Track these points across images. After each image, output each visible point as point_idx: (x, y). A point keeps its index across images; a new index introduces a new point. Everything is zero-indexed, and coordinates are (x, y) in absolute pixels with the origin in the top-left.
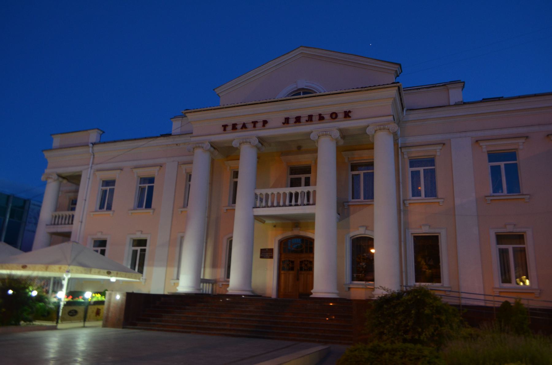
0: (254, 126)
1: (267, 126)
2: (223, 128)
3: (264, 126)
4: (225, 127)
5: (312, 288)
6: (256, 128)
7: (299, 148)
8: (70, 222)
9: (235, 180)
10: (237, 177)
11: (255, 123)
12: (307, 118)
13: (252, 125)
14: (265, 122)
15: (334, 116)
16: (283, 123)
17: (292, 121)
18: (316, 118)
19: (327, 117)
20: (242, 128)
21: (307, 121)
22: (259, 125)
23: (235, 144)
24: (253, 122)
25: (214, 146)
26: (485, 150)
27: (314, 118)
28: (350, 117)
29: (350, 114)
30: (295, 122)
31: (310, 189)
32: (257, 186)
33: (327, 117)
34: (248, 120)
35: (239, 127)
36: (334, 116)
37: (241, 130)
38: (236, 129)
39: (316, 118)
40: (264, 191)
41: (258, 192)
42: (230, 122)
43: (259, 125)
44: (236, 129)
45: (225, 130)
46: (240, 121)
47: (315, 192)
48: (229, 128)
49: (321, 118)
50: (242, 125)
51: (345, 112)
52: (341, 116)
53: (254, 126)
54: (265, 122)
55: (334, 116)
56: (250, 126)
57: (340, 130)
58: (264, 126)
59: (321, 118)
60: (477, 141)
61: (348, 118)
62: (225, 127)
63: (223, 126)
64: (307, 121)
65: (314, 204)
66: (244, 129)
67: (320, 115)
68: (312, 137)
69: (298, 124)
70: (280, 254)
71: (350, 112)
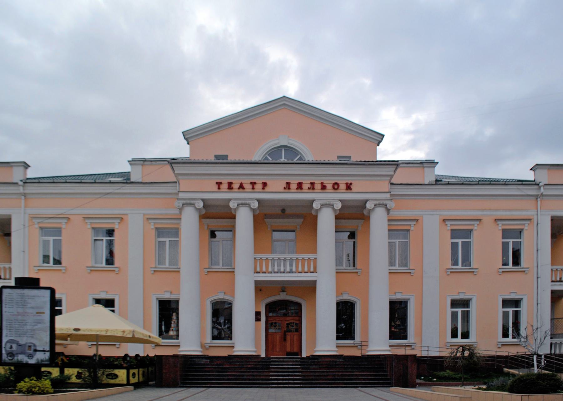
0: (253, 188)
1: (267, 189)
2: (217, 186)
3: (263, 189)
4: (219, 184)
5: (315, 347)
8: (8, 277)
11: (253, 184)
12: (309, 186)
13: (251, 186)
14: (265, 185)
15: (336, 186)
16: (285, 188)
17: (294, 186)
18: (318, 186)
19: (329, 186)
20: (239, 188)
21: (309, 188)
22: (259, 187)
23: (233, 205)
24: (251, 183)
25: (207, 204)
27: (316, 186)
28: (351, 189)
29: (352, 187)
30: (297, 189)
31: (312, 256)
32: (256, 251)
33: (329, 186)
34: (246, 182)
35: (236, 186)
37: (237, 190)
38: (232, 188)
39: (318, 186)
41: (259, 256)
43: (259, 187)
44: (232, 188)
45: (219, 188)
47: (316, 259)
48: (225, 186)
49: (324, 187)
50: (238, 185)
51: (347, 184)
52: (343, 187)
53: (253, 188)
55: (336, 187)
56: (248, 186)
57: (341, 200)
58: (263, 189)
61: (349, 191)
63: (217, 183)
64: (309, 188)
65: (315, 271)
66: (241, 190)
67: (322, 183)
68: (316, 205)
69: (299, 191)
71: (351, 184)
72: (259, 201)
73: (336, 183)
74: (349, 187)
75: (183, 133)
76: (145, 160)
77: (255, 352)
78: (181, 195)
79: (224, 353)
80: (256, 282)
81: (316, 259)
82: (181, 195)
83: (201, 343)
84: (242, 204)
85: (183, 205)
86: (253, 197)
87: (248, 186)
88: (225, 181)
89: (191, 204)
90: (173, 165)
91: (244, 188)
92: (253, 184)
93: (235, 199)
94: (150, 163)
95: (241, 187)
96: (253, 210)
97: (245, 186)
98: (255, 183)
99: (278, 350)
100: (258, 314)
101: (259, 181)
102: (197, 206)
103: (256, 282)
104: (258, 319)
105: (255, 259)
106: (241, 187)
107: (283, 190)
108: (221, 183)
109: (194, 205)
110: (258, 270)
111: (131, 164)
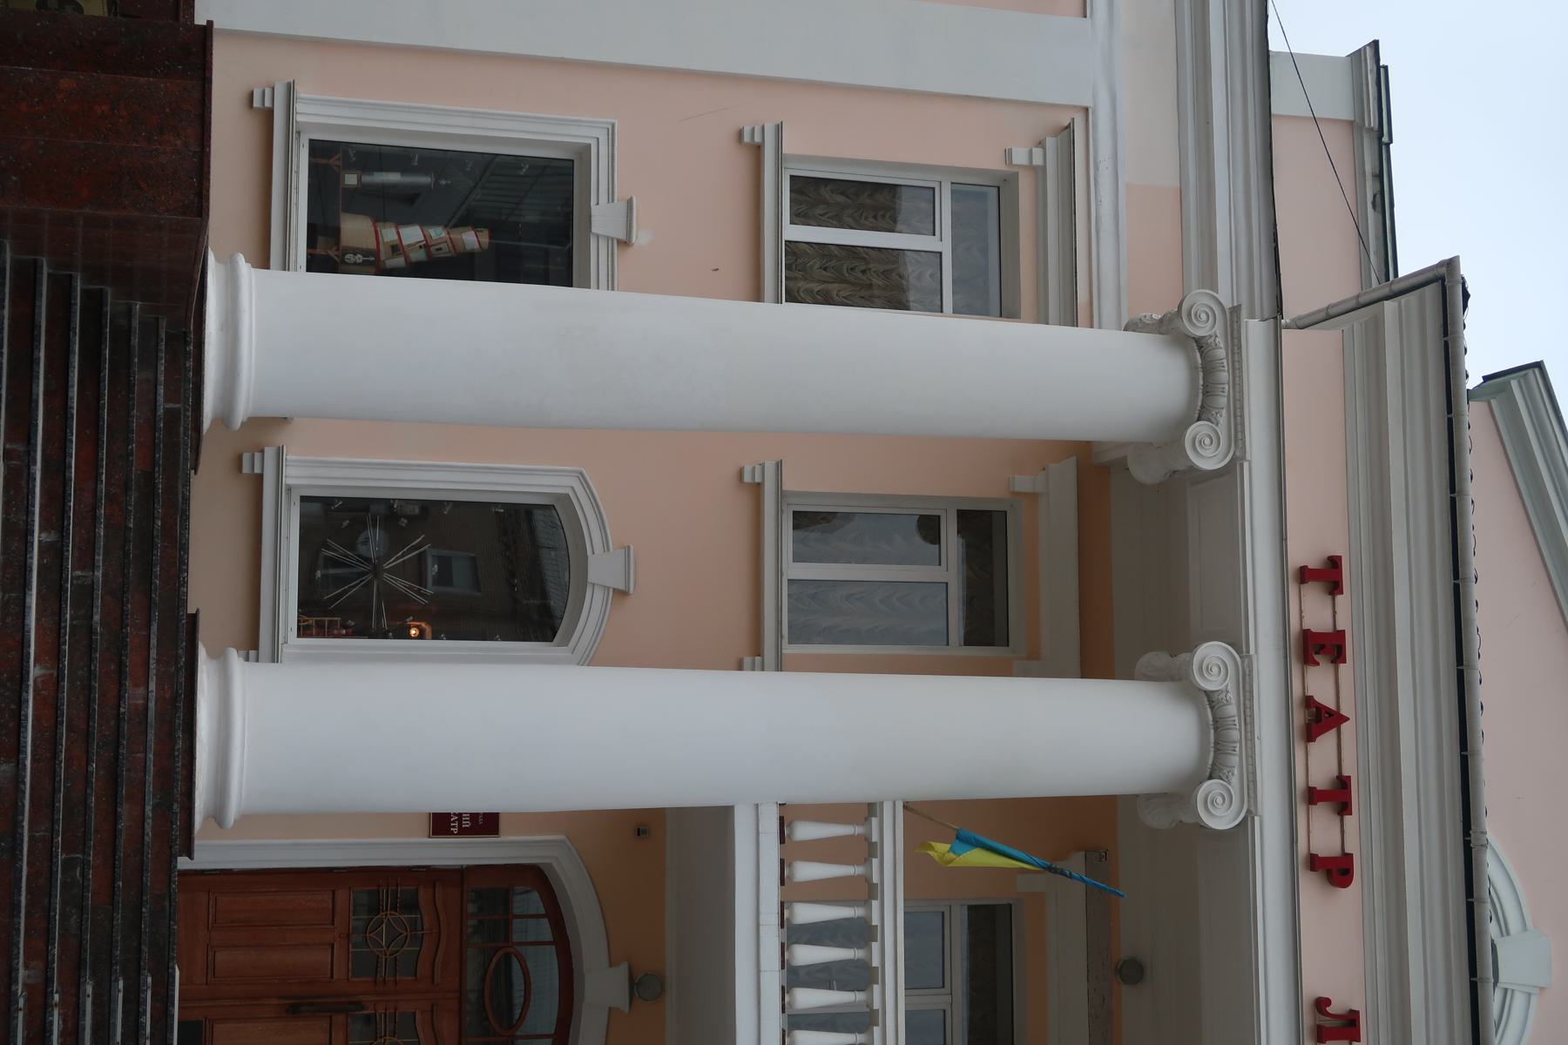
0: (1313, 796)
1: (1310, 886)
2: (1314, 562)
4: (1328, 576)
6: (1301, 810)
7: (1133, 971)
13: (1321, 776)
14: (1337, 871)
16: (1321, 1004)
20: (1309, 701)
22: (1323, 833)
24: (1343, 783)
35: (1320, 684)
38: (1307, 660)
40: (890, 871)
41: (890, 834)
43: (1323, 833)
45: (1305, 575)
48: (1316, 613)
50: (1325, 698)
53: (1313, 796)
56: (1320, 762)
58: (1315, 862)
63: (1334, 563)
66: (1299, 718)
70: (459, 876)
72: (1243, 830)
75: (1539, 366)
76: (1381, 139)
77: (217, 815)
78: (1255, 332)
79: (209, 585)
80: (717, 821)
82: (1255, 332)
83: (285, 420)
84: (1219, 724)
85: (1200, 343)
86: (1258, 800)
87: (1320, 762)
88: (1344, 613)
89: (1208, 390)
90: (1431, 292)
91: (1310, 734)
92: (1338, 796)
93: (1245, 681)
94: (1369, 167)
95: (1320, 720)
96: (1177, 795)
97: (1327, 741)
98: (1344, 808)
99: (222, 957)
100: (486, 824)
102: (1198, 429)
103: (717, 821)
104: (441, 824)
105: (871, 810)
106: (1320, 720)
107: (1314, 986)
108: (1335, 588)
109: (1203, 413)
110: (805, 831)
111: (1357, 56)
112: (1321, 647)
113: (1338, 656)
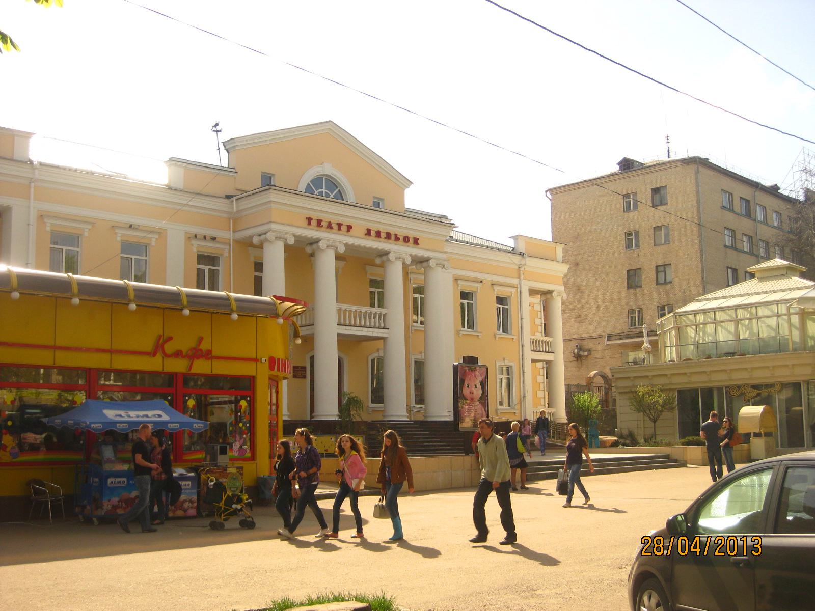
0: (340, 229)
2: (306, 222)
4: (309, 220)
9: (258, 274)
10: (261, 271)
11: (340, 225)
12: (385, 236)
14: (349, 228)
15: (406, 239)
20: (327, 228)
21: (385, 238)
26: (460, 288)
33: (401, 238)
34: (335, 220)
36: (406, 239)
37: (325, 229)
42: (315, 216)
43: (344, 228)
45: (309, 224)
46: (326, 218)
47: (384, 315)
48: (314, 223)
49: (397, 238)
53: (340, 229)
54: (349, 228)
56: (335, 227)
59: (397, 238)
60: (456, 279)
61: (415, 246)
62: (309, 220)
63: (307, 218)
64: (385, 238)
66: (329, 230)
67: (396, 235)
69: (377, 239)
71: (418, 239)
72: (347, 246)
73: (407, 237)
74: (416, 241)
81: (384, 315)
86: (341, 240)
97: (333, 225)
101: (346, 221)
103: (339, 335)
112: (319, 223)
113: (322, 221)
